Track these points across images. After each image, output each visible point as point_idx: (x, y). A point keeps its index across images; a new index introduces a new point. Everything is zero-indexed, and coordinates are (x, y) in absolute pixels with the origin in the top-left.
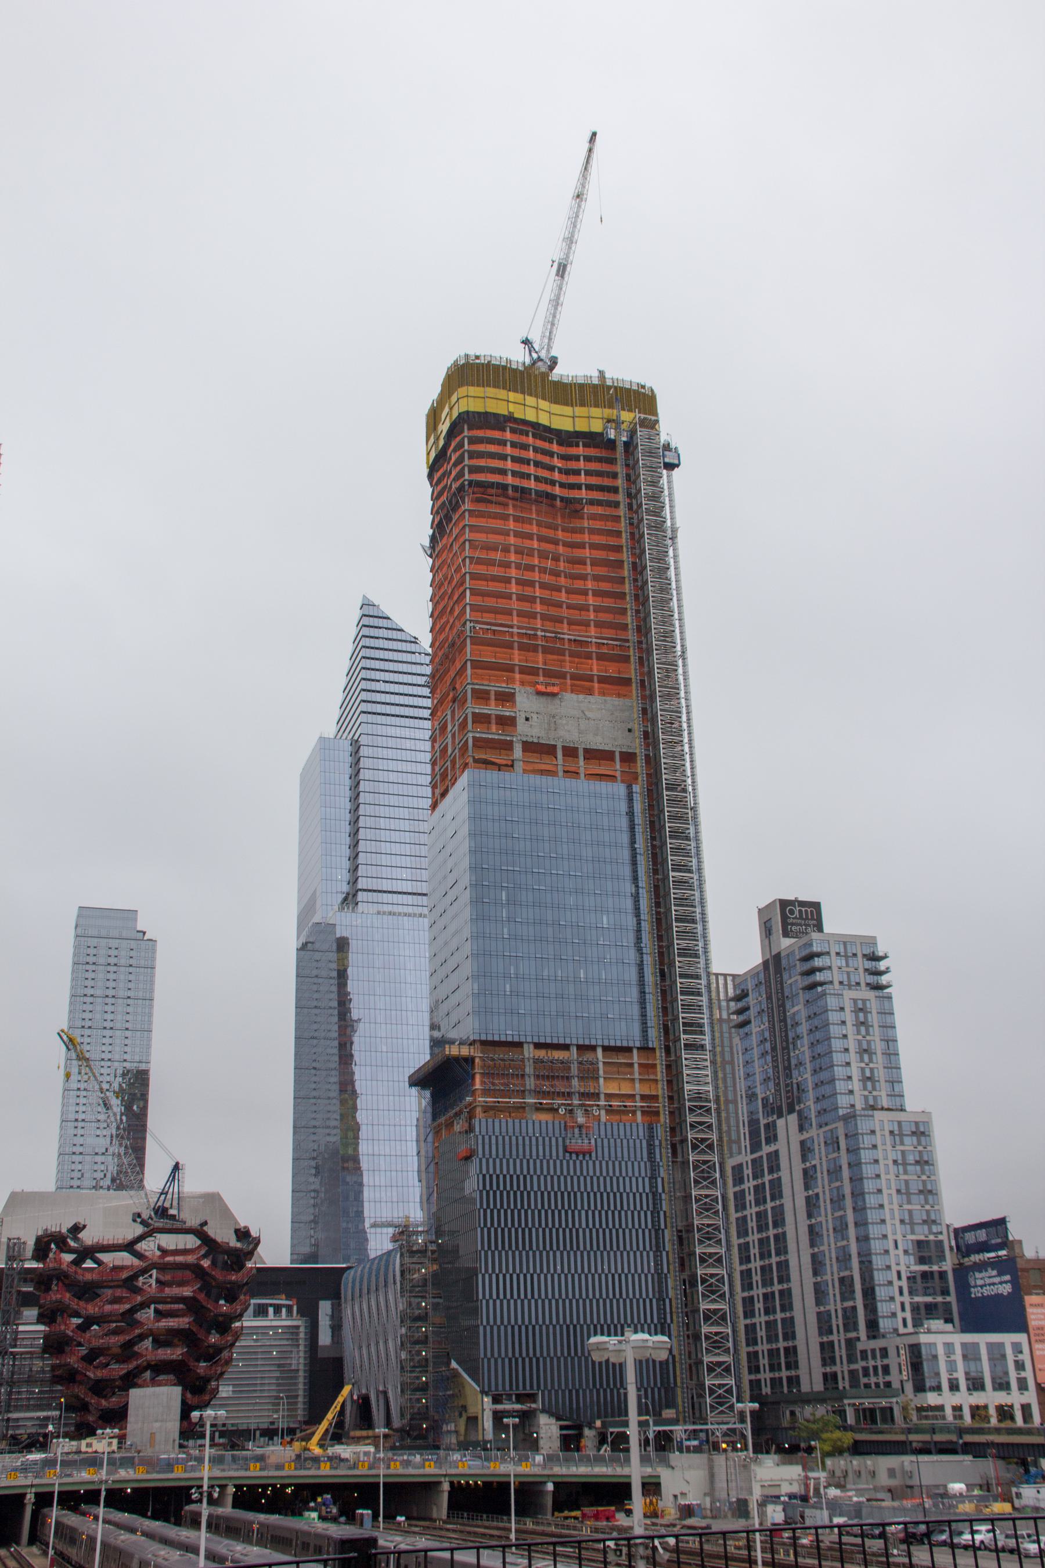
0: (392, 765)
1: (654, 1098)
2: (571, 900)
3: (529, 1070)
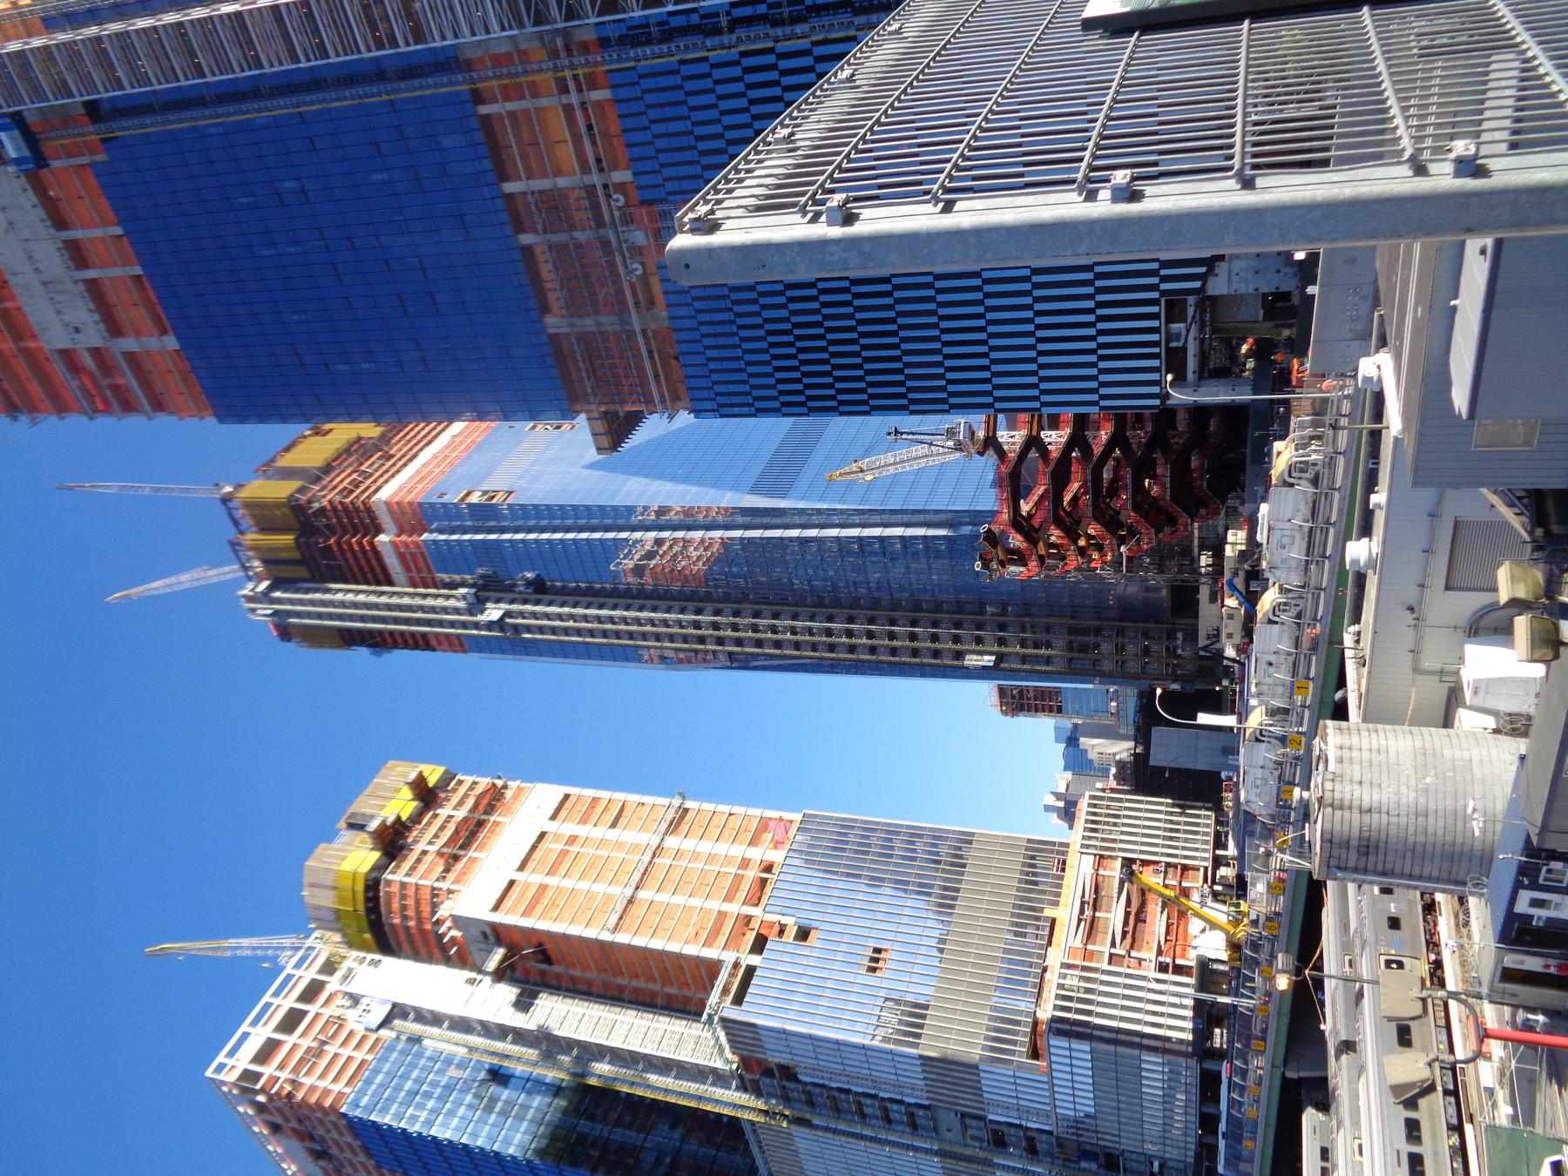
3: (588, 324)
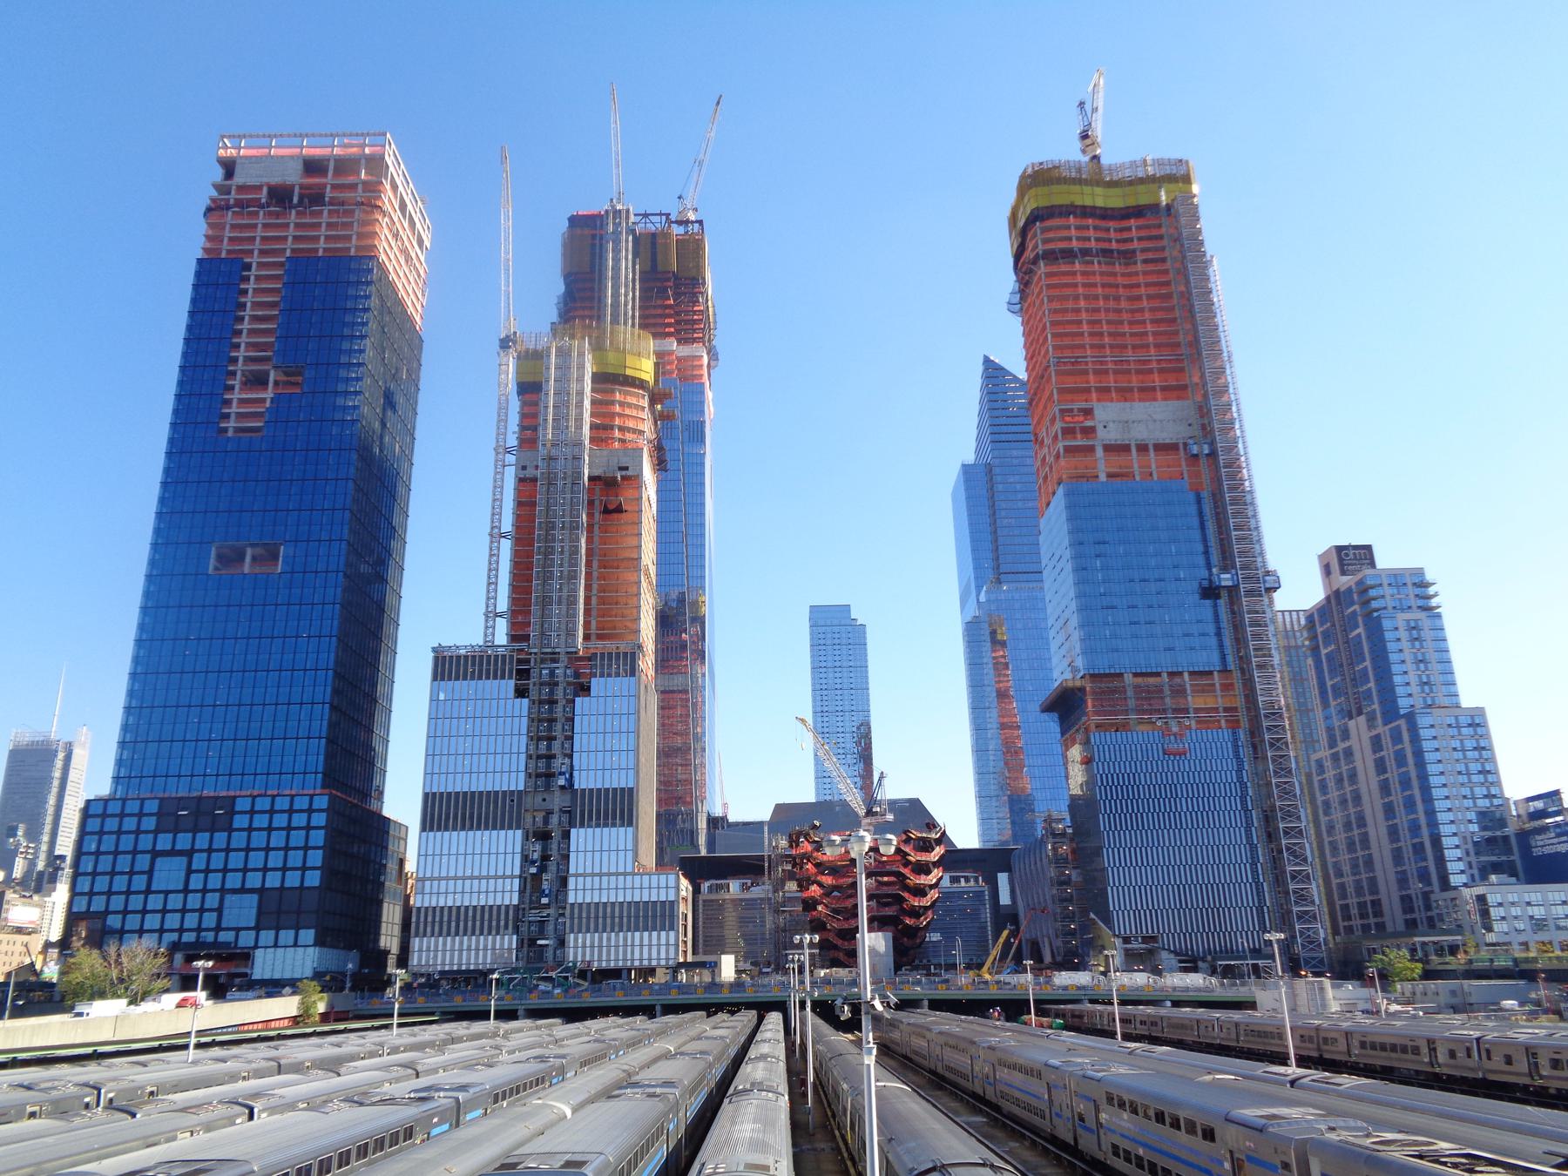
1: (1235, 709)
2: (1153, 562)
3: (1130, 693)
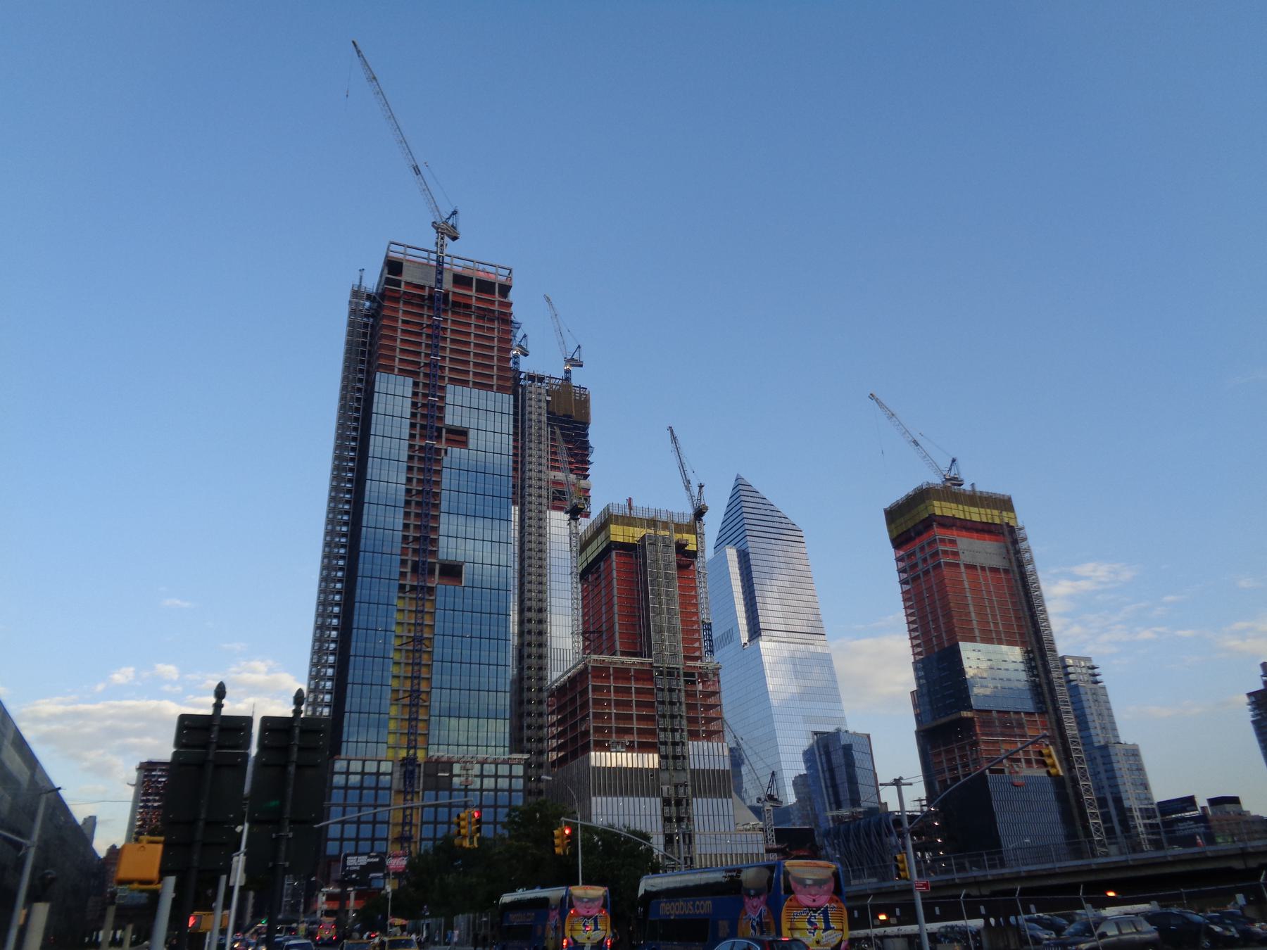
0: (765, 563)
